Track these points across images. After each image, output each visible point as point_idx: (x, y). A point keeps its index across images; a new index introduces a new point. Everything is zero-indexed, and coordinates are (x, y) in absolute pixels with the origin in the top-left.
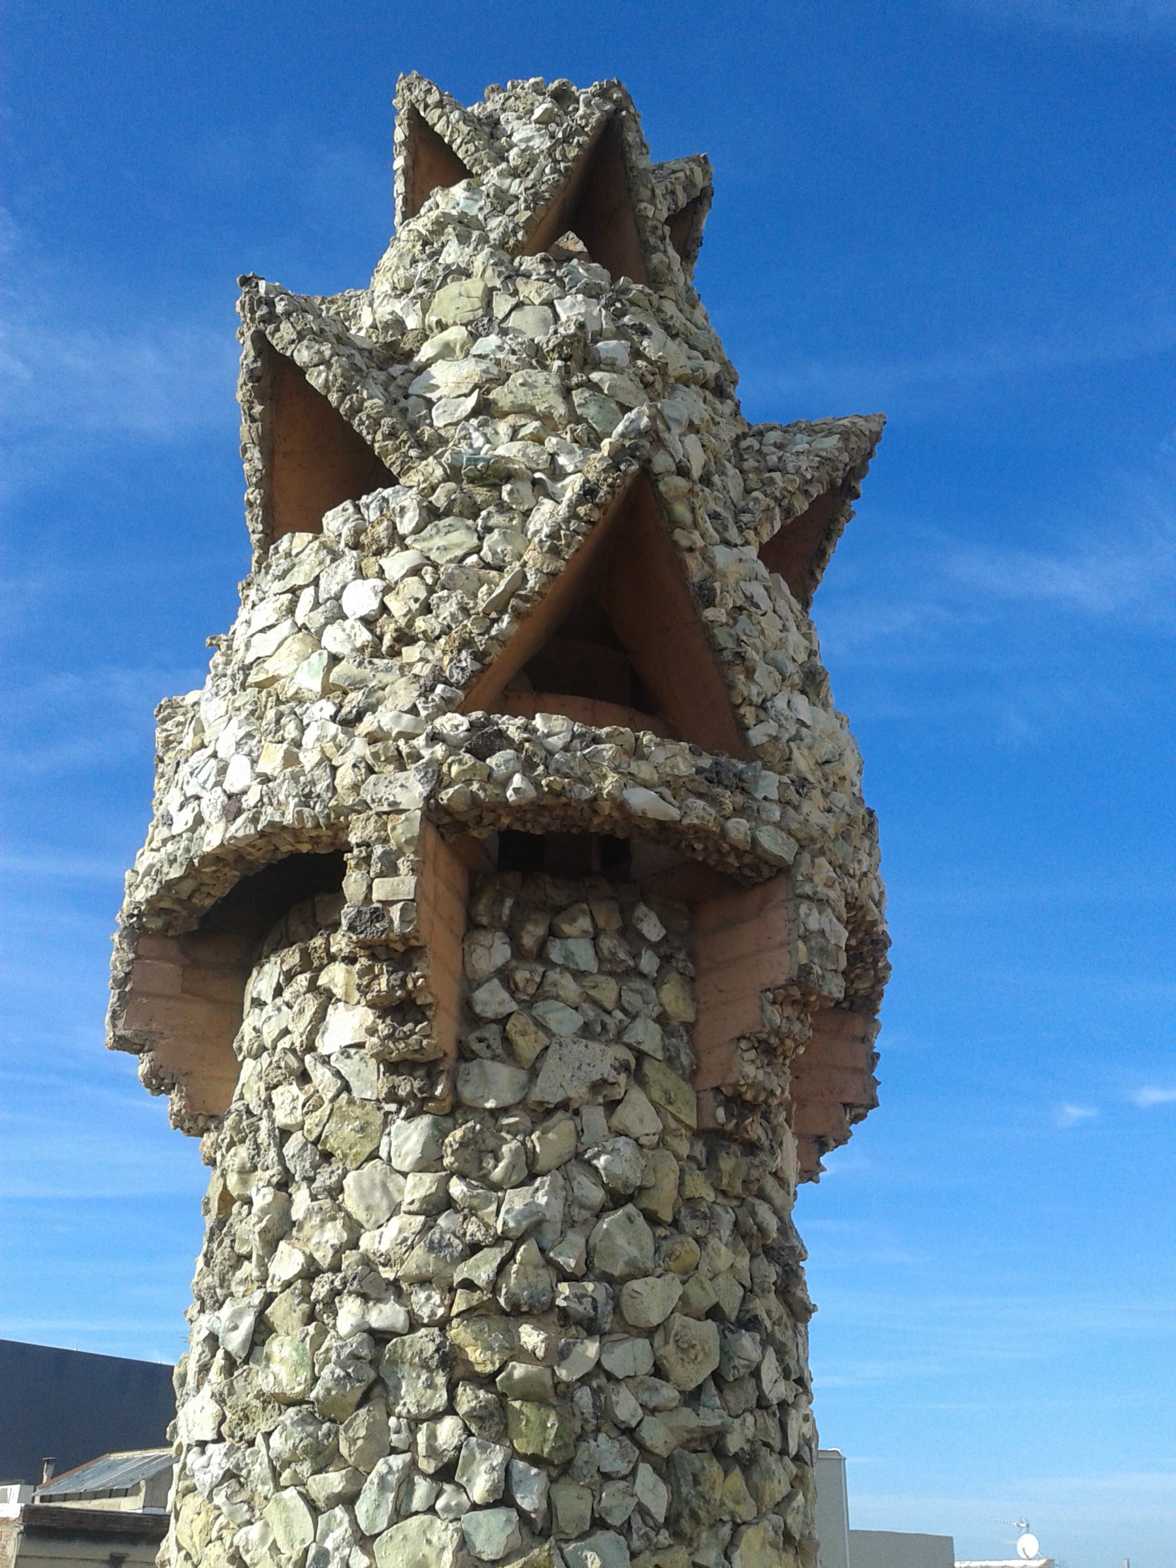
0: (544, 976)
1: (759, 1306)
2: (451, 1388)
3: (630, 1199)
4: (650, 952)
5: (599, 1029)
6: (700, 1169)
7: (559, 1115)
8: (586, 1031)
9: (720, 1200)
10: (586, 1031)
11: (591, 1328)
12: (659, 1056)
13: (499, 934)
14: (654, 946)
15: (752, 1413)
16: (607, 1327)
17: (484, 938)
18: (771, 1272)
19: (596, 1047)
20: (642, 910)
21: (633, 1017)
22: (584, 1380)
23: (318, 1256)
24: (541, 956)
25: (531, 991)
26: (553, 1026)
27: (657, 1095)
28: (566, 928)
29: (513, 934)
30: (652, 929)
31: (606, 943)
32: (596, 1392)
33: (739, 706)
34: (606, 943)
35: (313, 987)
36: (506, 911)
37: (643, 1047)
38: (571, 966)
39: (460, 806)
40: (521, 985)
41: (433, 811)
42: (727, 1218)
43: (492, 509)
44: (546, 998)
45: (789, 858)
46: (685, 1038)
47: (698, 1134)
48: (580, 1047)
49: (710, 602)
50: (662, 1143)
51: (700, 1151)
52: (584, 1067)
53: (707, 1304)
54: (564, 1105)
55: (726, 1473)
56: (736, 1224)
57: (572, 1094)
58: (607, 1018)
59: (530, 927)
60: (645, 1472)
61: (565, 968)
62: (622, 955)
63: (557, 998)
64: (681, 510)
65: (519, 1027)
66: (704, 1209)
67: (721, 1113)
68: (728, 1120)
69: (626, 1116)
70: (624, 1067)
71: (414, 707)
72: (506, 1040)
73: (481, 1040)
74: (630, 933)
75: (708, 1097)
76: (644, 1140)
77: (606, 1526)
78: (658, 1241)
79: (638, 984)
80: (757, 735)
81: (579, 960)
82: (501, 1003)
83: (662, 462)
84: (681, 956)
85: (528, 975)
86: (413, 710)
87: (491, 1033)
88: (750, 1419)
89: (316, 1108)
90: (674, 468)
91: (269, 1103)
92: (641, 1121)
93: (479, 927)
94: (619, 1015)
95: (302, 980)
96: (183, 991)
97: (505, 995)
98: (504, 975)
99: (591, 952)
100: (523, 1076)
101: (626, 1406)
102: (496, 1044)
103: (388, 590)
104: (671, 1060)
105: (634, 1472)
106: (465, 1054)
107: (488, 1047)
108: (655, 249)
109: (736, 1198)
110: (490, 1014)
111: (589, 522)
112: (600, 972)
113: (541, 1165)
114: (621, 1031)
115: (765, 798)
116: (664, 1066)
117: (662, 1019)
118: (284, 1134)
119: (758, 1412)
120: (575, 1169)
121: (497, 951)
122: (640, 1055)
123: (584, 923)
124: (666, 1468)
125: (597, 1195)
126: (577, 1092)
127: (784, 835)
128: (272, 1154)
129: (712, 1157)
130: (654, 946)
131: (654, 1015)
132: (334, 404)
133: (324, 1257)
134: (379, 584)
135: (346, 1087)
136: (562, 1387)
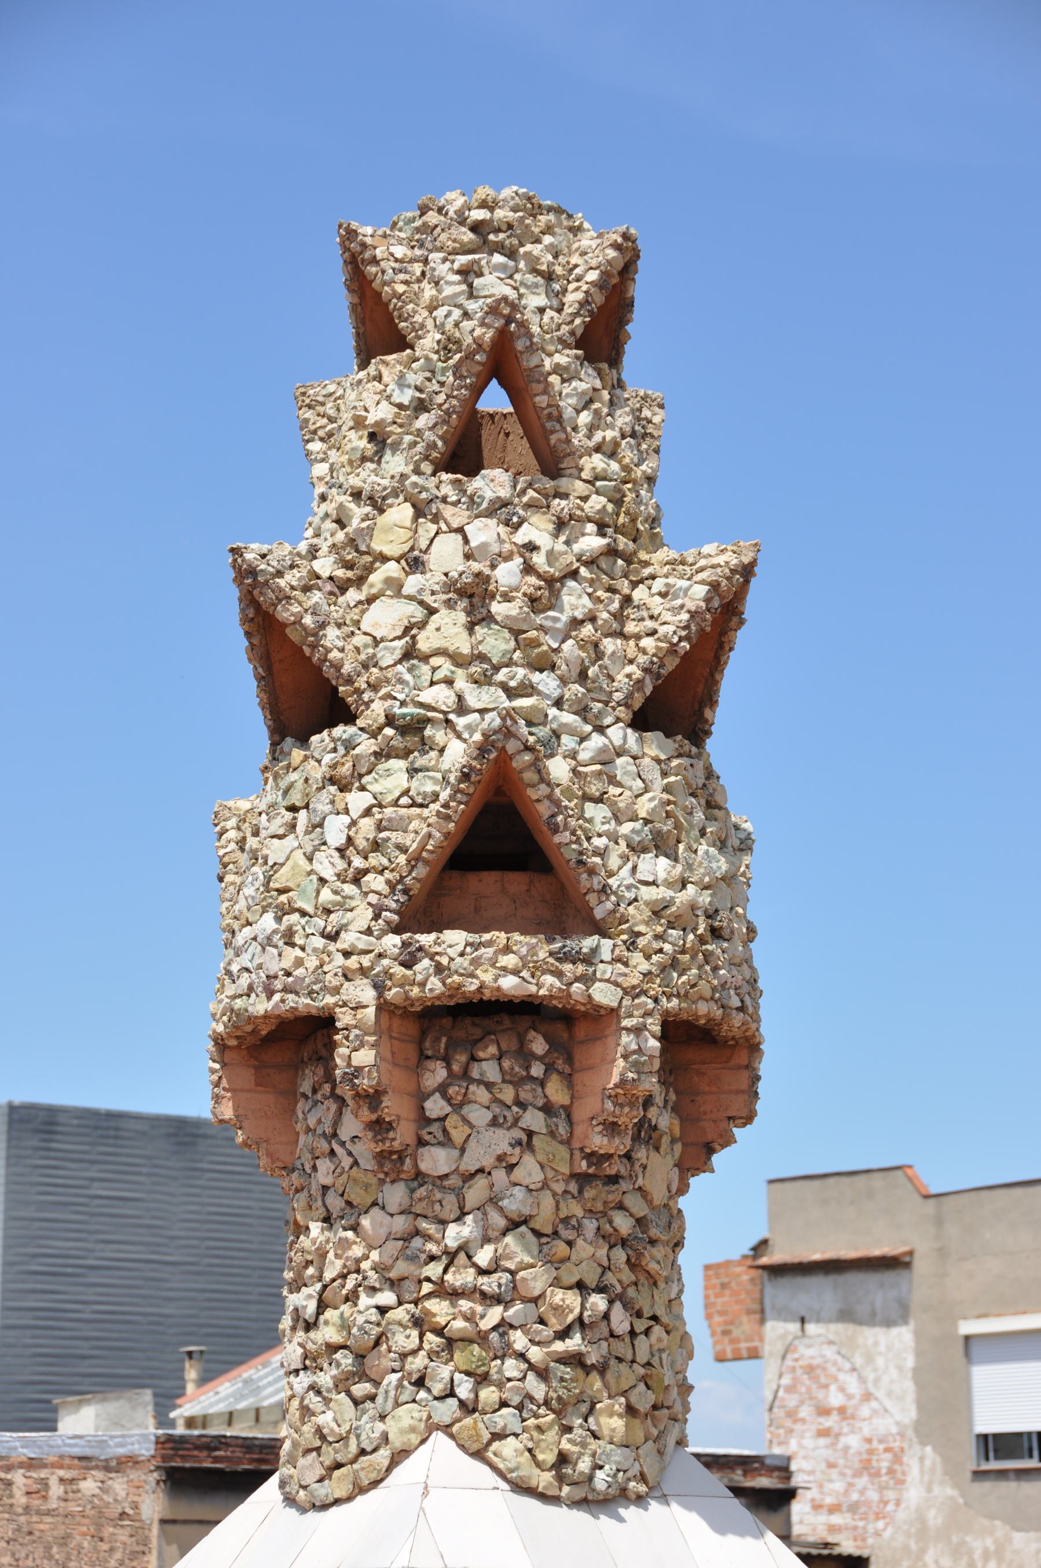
0: (467, 1088)
1: (610, 1278)
2: (421, 1336)
3: (525, 1222)
4: (538, 1063)
5: (501, 1120)
6: (574, 1197)
7: (479, 1176)
8: (494, 1123)
10: (494, 1123)
11: (497, 1299)
12: (544, 1131)
13: (438, 1062)
14: (541, 1059)
15: (606, 1339)
16: (509, 1299)
17: (431, 1064)
18: (620, 1255)
19: (500, 1132)
20: (532, 1034)
22: (494, 1329)
24: (465, 1075)
25: (460, 1098)
27: (541, 1157)
28: (481, 1054)
29: (447, 1060)
30: (539, 1046)
31: (506, 1064)
32: (502, 1335)
33: (585, 894)
36: (443, 1045)
39: (398, 1001)
40: (454, 1096)
41: (383, 1007)
42: (590, 1226)
43: (416, 754)
44: (470, 1102)
46: (563, 1116)
47: (573, 1176)
49: (556, 829)
50: (545, 1185)
51: (573, 1187)
52: (493, 1146)
53: (574, 1279)
54: (481, 1170)
55: (588, 1374)
56: (598, 1229)
57: (484, 1164)
58: (507, 1113)
60: (531, 1376)
61: (479, 1082)
62: (517, 1069)
63: (475, 1102)
64: (530, 776)
65: (453, 1123)
66: (574, 1222)
67: (584, 1163)
68: (589, 1167)
69: (518, 1174)
70: (519, 1143)
71: (369, 928)
72: (445, 1131)
73: (430, 1133)
75: (577, 1153)
76: (532, 1187)
77: (509, 1406)
78: (541, 1245)
80: (599, 913)
81: (488, 1075)
83: (512, 746)
84: (560, 1061)
85: (457, 1088)
86: (369, 932)
87: (435, 1128)
88: (604, 1344)
89: (341, 1174)
90: (522, 747)
91: (314, 1168)
92: (530, 1175)
93: (428, 1058)
94: (515, 1109)
96: (257, 1085)
97: (443, 1103)
98: (442, 1089)
99: (498, 1068)
100: (456, 1153)
101: (519, 1340)
102: (440, 1136)
103: (354, 823)
104: (552, 1134)
105: (525, 1377)
106: (421, 1143)
108: (553, 432)
109: (600, 1212)
111: (468, 794)
112: (504, 1081)
113: (466, 1210)
114: (516, 1120)
116: (548, 1139)
117: (548, 1109)
118: (325, 1188)
119: (611, 1340)
120: (489, 1209)
121: (436, 1074)
122: (530, 1134)
123: (492, 1049)
124: (543, 1374)
125: (502, 1223)
126: (488, 1162)
127: (613, 988)
128: (320, 1203)
129: (581, 1191)
130: (541, 1059)
131: (540, 1105)
132: (308, 655)
134: (346, 820)
135: (356, 1163)
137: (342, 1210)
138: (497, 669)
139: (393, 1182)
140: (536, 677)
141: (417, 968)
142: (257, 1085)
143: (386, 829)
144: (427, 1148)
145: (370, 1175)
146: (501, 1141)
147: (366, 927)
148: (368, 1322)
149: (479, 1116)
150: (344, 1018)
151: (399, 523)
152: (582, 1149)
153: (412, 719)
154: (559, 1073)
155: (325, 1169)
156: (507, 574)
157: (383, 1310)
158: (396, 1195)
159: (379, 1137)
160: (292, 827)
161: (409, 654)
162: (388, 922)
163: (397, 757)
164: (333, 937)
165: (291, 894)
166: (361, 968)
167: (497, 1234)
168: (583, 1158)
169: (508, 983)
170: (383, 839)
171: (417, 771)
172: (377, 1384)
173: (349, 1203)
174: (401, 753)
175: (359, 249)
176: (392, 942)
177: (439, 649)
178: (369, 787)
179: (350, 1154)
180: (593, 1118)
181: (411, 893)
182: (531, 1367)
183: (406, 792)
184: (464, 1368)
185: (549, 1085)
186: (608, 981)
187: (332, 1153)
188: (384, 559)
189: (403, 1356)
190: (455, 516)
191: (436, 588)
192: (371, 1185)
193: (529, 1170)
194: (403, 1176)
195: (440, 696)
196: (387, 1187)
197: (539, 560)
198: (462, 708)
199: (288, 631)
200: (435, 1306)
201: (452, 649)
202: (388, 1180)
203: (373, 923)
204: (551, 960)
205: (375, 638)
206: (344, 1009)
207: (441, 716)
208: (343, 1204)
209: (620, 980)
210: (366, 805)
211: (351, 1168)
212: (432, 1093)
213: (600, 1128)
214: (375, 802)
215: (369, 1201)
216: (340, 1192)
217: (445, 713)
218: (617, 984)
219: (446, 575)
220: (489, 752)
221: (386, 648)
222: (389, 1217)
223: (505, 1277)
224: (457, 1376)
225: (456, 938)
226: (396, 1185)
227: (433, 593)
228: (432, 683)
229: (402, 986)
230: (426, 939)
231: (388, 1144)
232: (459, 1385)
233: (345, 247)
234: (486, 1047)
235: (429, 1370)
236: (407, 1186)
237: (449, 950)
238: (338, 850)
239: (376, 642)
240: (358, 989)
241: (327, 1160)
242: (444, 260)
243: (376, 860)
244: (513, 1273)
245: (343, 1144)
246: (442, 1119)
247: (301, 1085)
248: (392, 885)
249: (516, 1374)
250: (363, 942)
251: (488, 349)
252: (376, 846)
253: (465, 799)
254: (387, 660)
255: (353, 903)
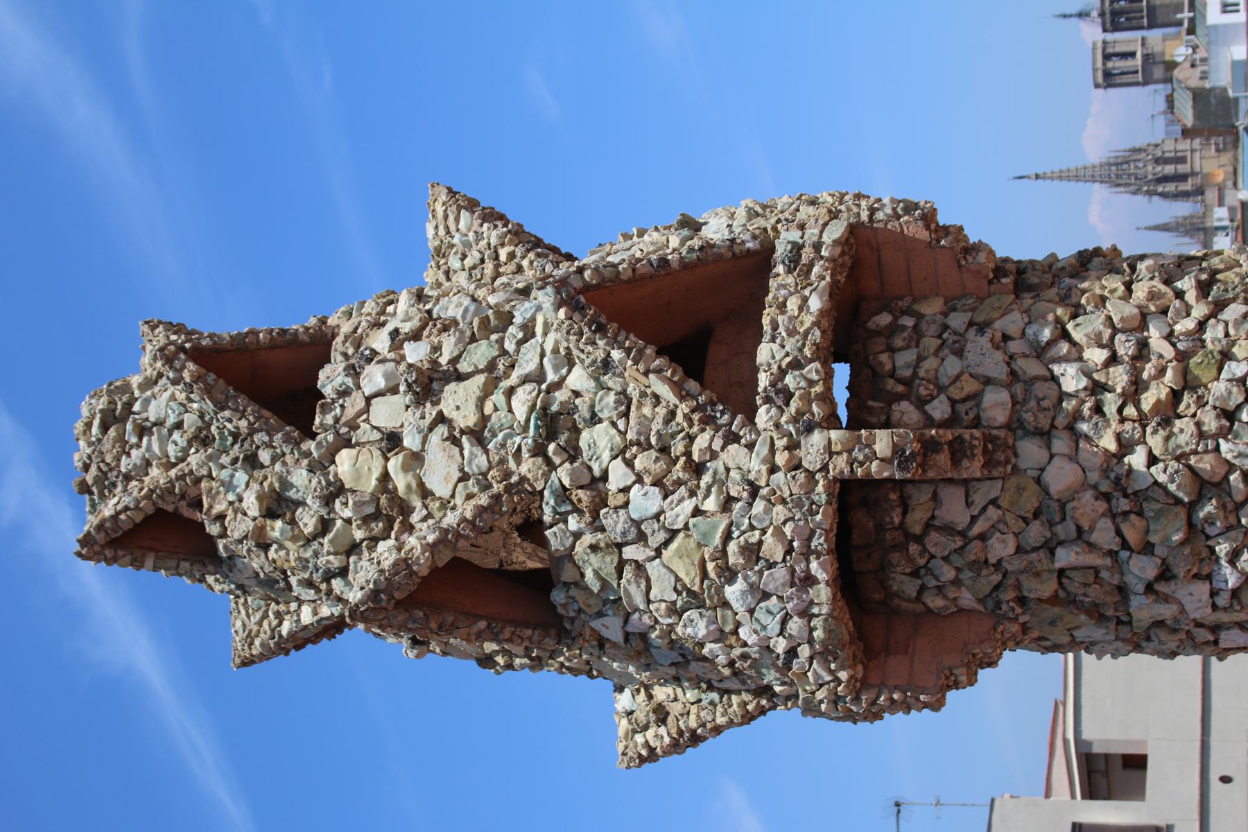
0: (922, 379)
5: (957, 345)
8: (959, 353)
9: (1057, 285)
10: (959, 353)
12: (970, 314)
13: (893, 407)
14: (896, 318)
17: (896, 416)
19: (969, 346)
20: (871, 325)
21: (946, 327)
22: (1174, 345)
23: (1101, 510)
25: (932, 387)
26: (956, 372)
27: (996, 314)
28: (888, 367)
30: (884, 319)
34: (899, 342)
35: (919, 539)
36: (876, 404)
37: (967, 321)
38: (914, 363)
44: (937, 378)
45: (845, 224)
48: (970, 356)
50: (1027, 311)
52: (983, 352)
56: (1071, 277)
57: (1001, 358)
59: (889, 388)
63: (937, 371)
65: (958, 391)
67: (1004, 280)
69: (1013, 330)
72: (964, 400)
73: (967, 414)
74: (894, 329)
76: (1026, 320)
79: (924, 326)
81: (910, 360)
82: (941, 402)
84: (900, 303)
85: (921, 388)
86: (750, 446)
87: (961, 408)
92: (1013, 322)
93: (888, 418)
94: (945, 335)
95: (914, 548)
96: (906, 652)
97: (935, 402)
99: (903, 352)
100: (989, 388)
101: (1188, 324)
102: (969, 404)
104: (973, 310)
106: (976, 423)
107: (971, 409)
110: (949, 410)
112: (917, 346)
115: (802, 238)
122: (971, 324)
123: (884, 358)
128: (1034, 556)
129: (1030, 288)
130: (896, 318)
133: (1101, 506)
135: (994, 502)
136: (1178, 357)
137: (1043, 524)
138: (504, 353)
139: (1016, 455)
140: (518, 320)
141: (792, 387)
142: (906, 652)
143: (648, 439)
144: (981, 414)
145: (1007, 485)
146: (978, 345)
147: (746, 450)
148: (1165, 472)
149: (952, 366)
150: (840, 464)
151: (354, 461)
152: (990, 282)
153: (541, 421)
154: (912, 304)
155: (1001, 548)
156: (415, 353)
157: (1152, 460)
158: (1030, 451)
159: (969, 453)
160: (639, 567)
161: (478, 435)
162: (743, 425)
163: (577, 440)
164: (754, 490)
165: (707, 557)
166: (787, 448)
167: (1074, 350)
168: (999, 281)
169: (815, 303)
170: (658, 440)
171: (594, 415)
172: (1231, 467)
173: (1036, 515)
174: (574, 436)
175: (103, 534)
176: (763, 416)
177: (477, 406)
178: (604, 465)
179: (984, 509)
180: (960, 266)
181: (715, 399)
182: (1213, 315)
183: (614, 424)
184: (1214, 372)
185: (923, 312)
186: (821, 232)
187: (983, 537)
188: (385, 477)
189: (1201, 435)
190: (355, 403)
191: (418, 415)
192: (1018, 483)
193: (1012, 322)
194: (1010, 441)
195: (521, 402)
196: (1022, 465)
197: (406, 328)
198: (538, 377)
199: (441, 564)
200: (1148, 400)
201: (478, 393)
202: (1013, 460)
203: (743, 441)
204: (795, 274)
205: (460, 480)
206: (831, 467)
207: (542, 395)
208: (1037, 522)
209: (821, 222)
210: (623, 466)
211: (999, 507)
212: (925, 413)
213: (970, 259)
214: (620, 458)
215: (1035, 487)
216: (1024, 525)
217: (540, 392)
218: (825, 225)
219: (408, 407)
220: (578, 302)
221: (470, 463)
222: (1055, 460)
223: (1120, 337)
224: (1224, 375)
225: (764, 352)
226: (1019, 451)
227: (423, 417)
228: (510, 410)
229: (810, 402)
230: (763, 380)
231: (976, 443)
232: (1234, 375)
233: (99, 553)
234: (881, 363)
235: (1217, 404)
236: (1022, 438)
237: (778, 358)
238: (665, 497)
239: (464, 477)
240: (811, 451)
241: (990, 542)
242: (128, 454)
243: (678, 447)
244: (1115, 331)
245: (974, 519)
246: (953, 402)
247: (909, 595)
248: (708, 421)
249: (1221, 327)
250: (762, 449)
251: (203, 371)
252: (664, 450)
253: (623, 333)
254: (482, 461)
255: (721, 469)
